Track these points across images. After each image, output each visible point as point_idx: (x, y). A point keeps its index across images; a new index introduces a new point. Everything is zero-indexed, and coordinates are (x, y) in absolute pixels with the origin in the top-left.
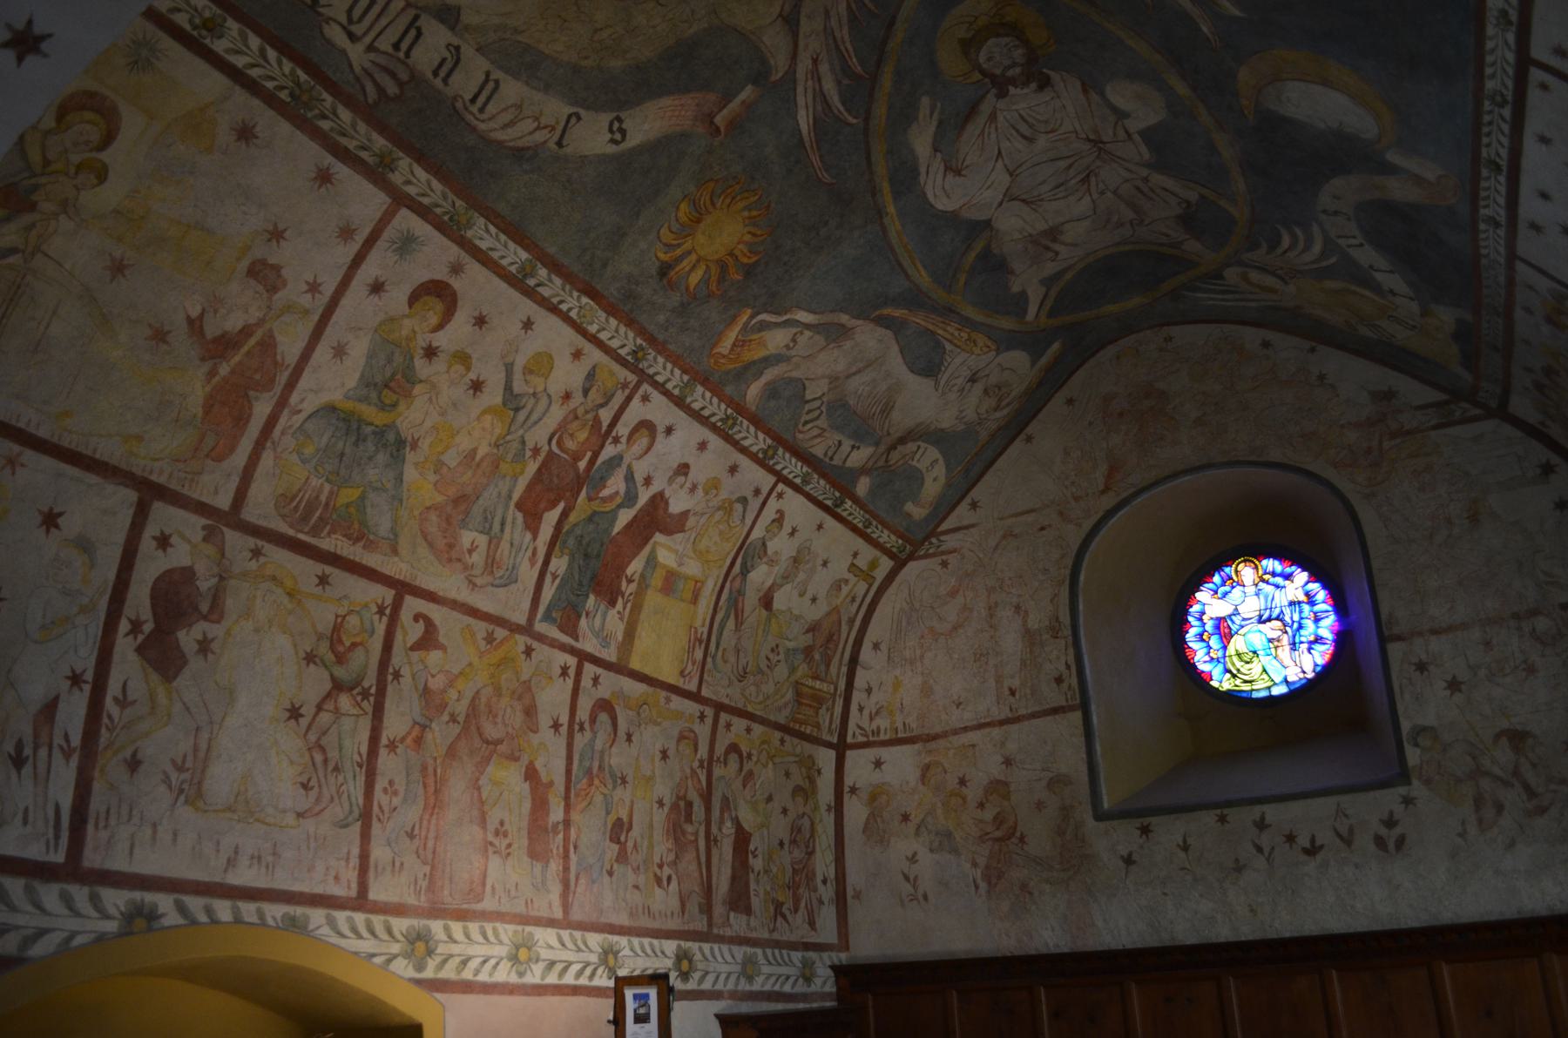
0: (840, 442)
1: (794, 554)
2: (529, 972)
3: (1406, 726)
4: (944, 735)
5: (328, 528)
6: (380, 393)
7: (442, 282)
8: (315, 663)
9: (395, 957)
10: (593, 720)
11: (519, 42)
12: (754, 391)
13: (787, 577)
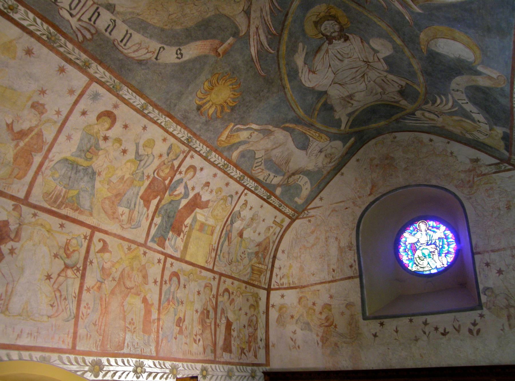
0: (269, 175)
1: (252, 217)
2: (141, 376)
3: (481, 287)
4: (307, 286)
5: (64, 205)
6: (86, 154)
7: (110, 111)
8: (58, 258)
9: (86, 372)
10: (170, 280)
11: (139, 19)
12: (235, 155)
13: (249, 225)
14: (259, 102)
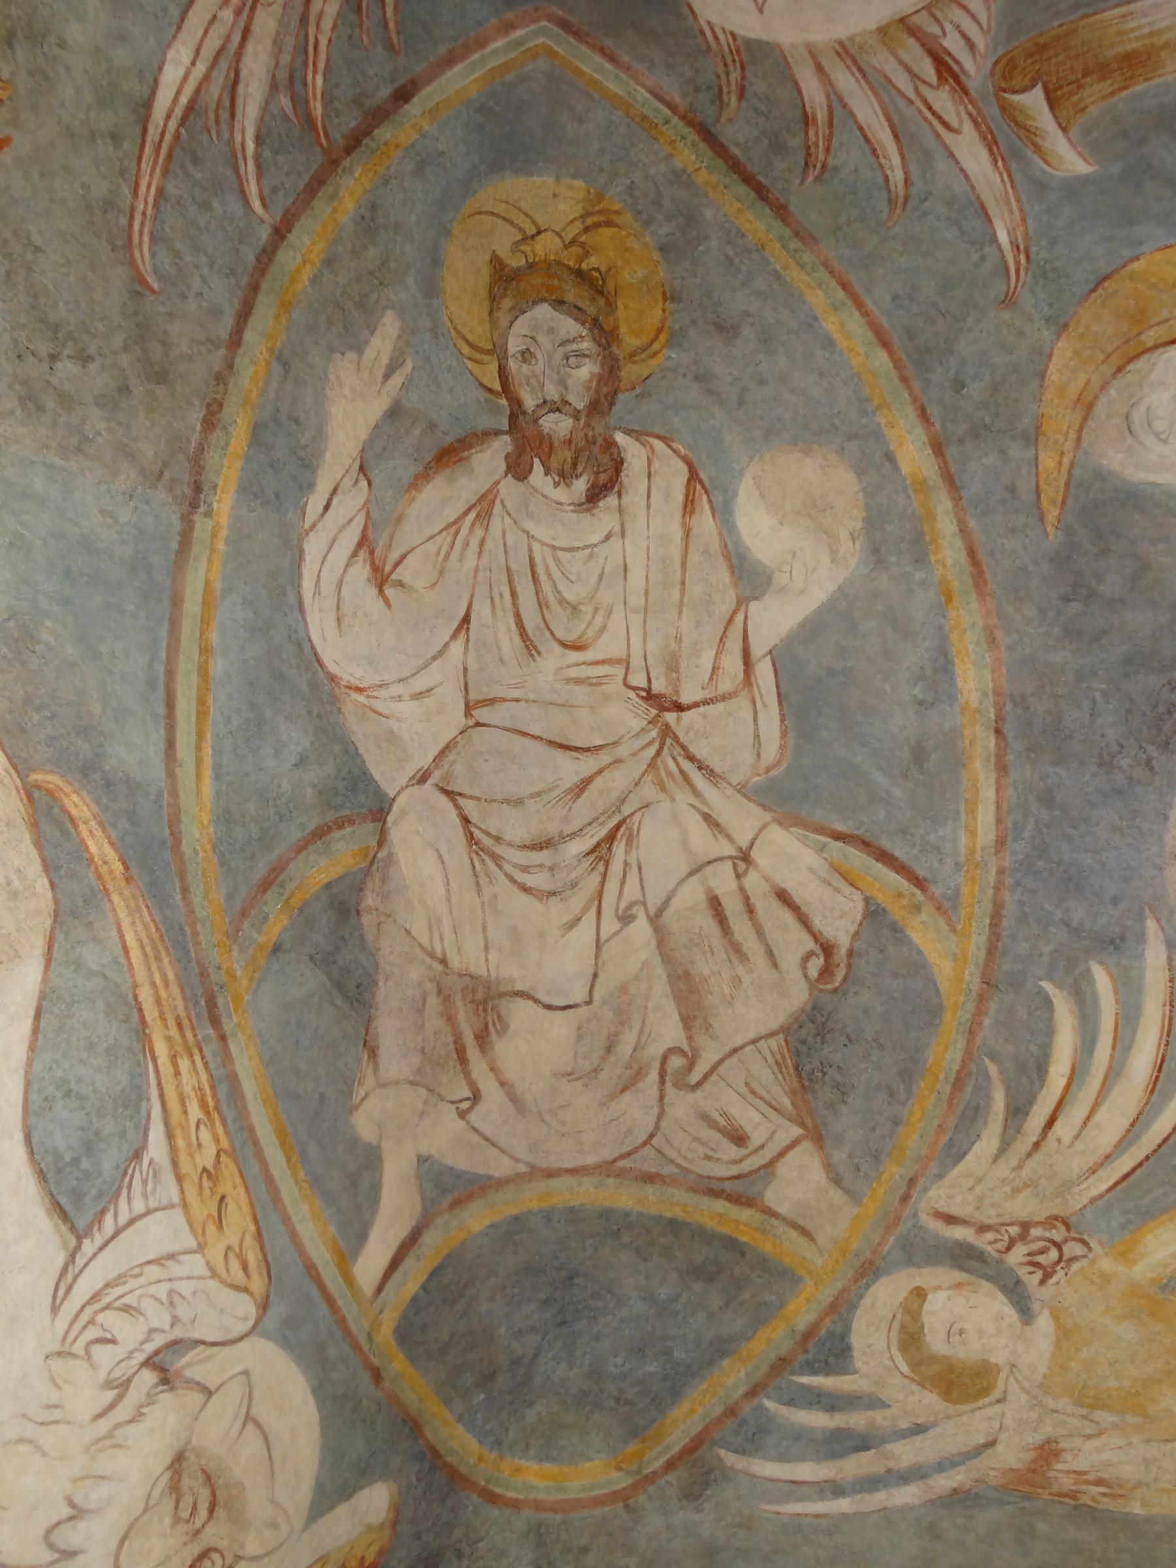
14: (22, 400)
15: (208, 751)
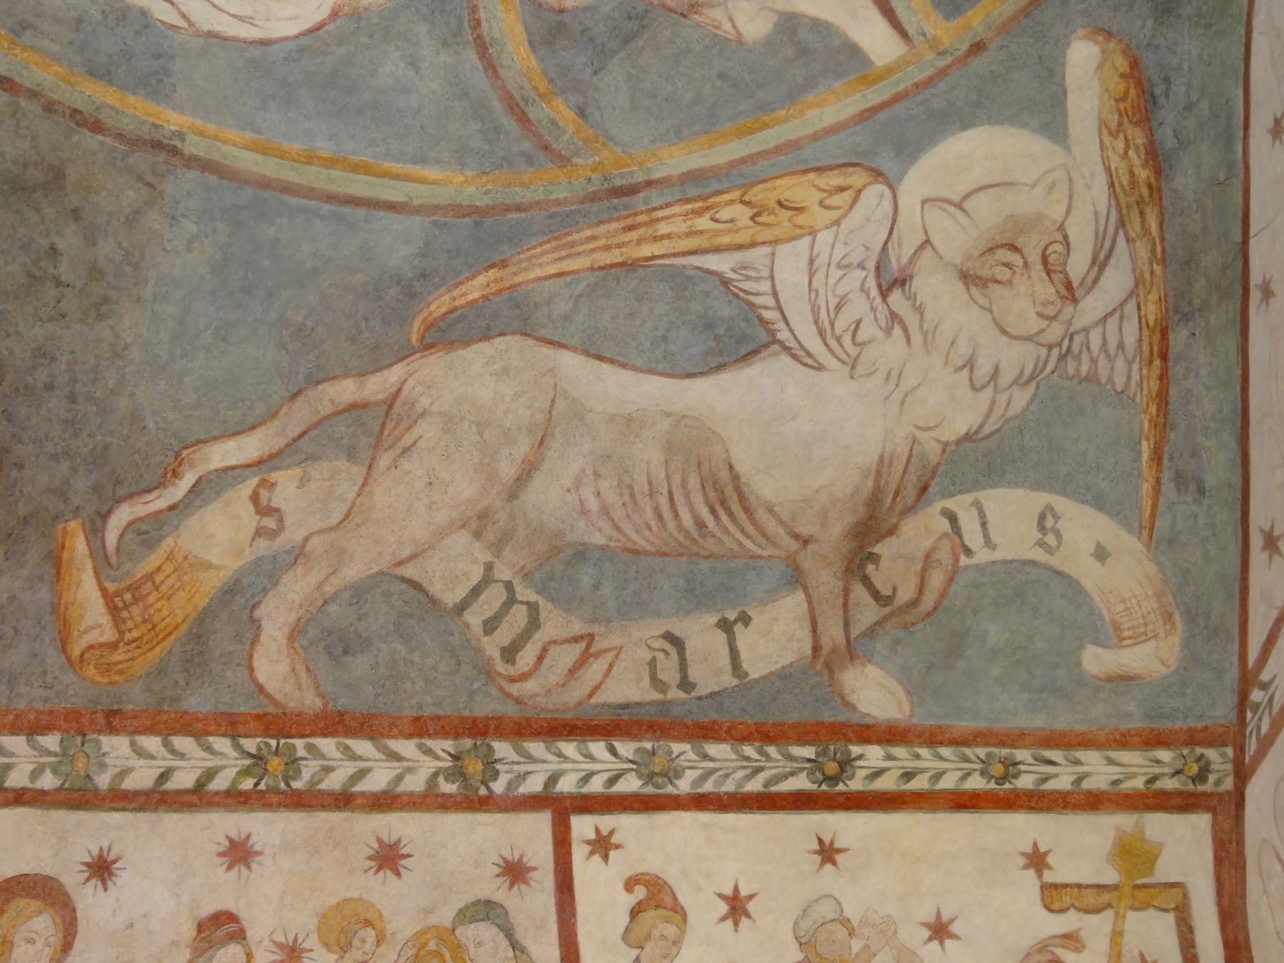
0: (676, 642)
14: (100, 317)
15: (397, 167)
